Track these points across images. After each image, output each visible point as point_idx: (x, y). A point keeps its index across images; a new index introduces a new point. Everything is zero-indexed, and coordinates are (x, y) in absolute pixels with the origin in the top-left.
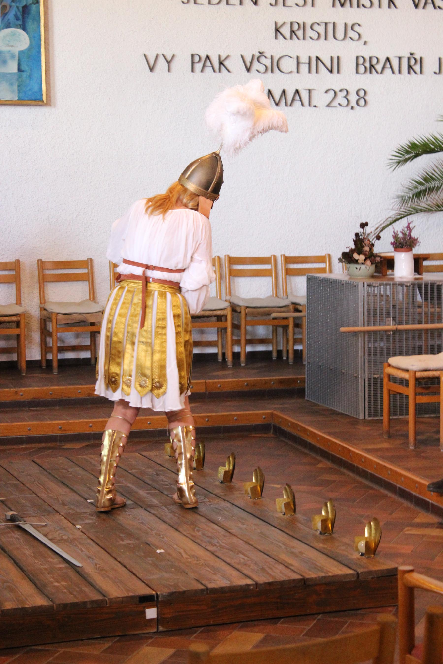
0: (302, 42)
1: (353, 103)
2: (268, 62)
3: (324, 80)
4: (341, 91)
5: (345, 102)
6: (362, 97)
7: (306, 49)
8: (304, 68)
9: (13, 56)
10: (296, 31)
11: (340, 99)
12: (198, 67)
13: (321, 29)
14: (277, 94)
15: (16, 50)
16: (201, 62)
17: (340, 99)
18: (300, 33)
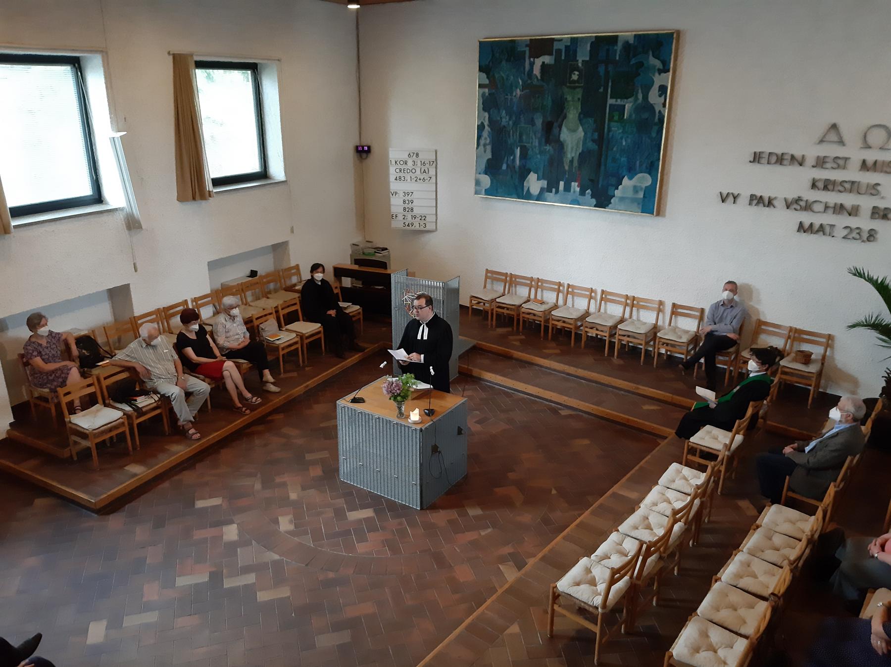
0: (833, 193)
1: (865, 239)
2: (803, 204)
3: (841, 221)
4: (858, 228)
5: (858, 237)
6: (872, 236)
7: (832, 198)
8: (830, 211)
9: (641, 189)
10: (828, 185)
11: (854, 235)
12: (755, 202)
13: (847, 186)
14: (806, 225)
15: (644, 186)
16: (757, 200)
17: (854, 235)
18: (830, 187)
